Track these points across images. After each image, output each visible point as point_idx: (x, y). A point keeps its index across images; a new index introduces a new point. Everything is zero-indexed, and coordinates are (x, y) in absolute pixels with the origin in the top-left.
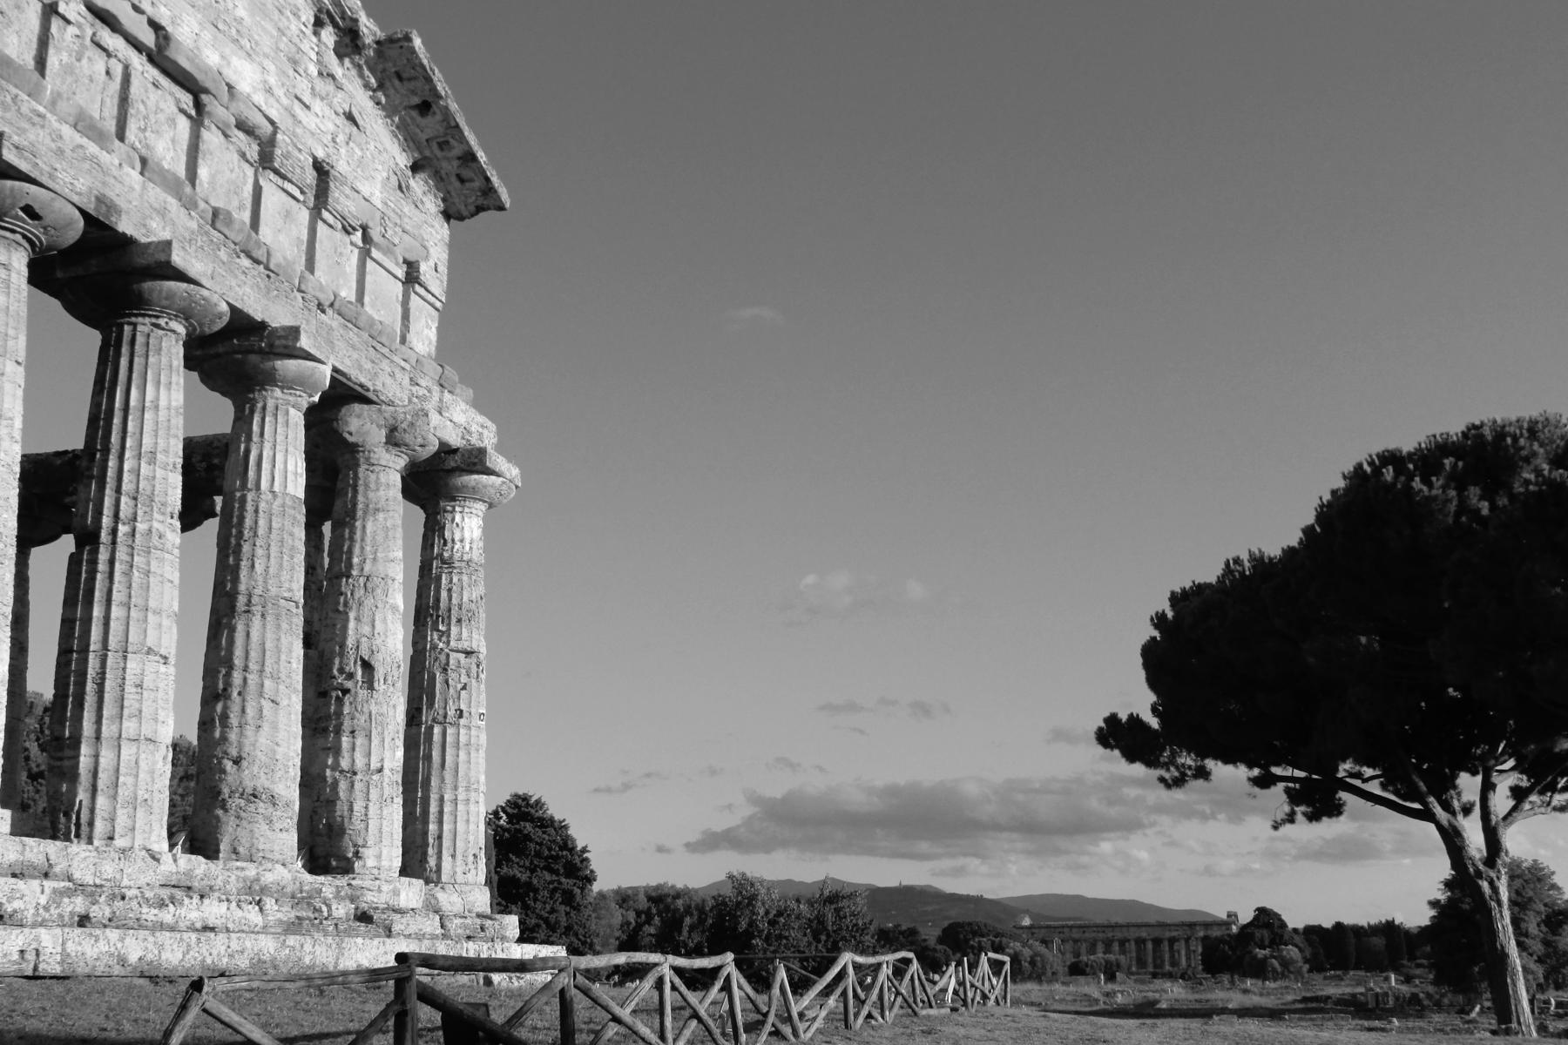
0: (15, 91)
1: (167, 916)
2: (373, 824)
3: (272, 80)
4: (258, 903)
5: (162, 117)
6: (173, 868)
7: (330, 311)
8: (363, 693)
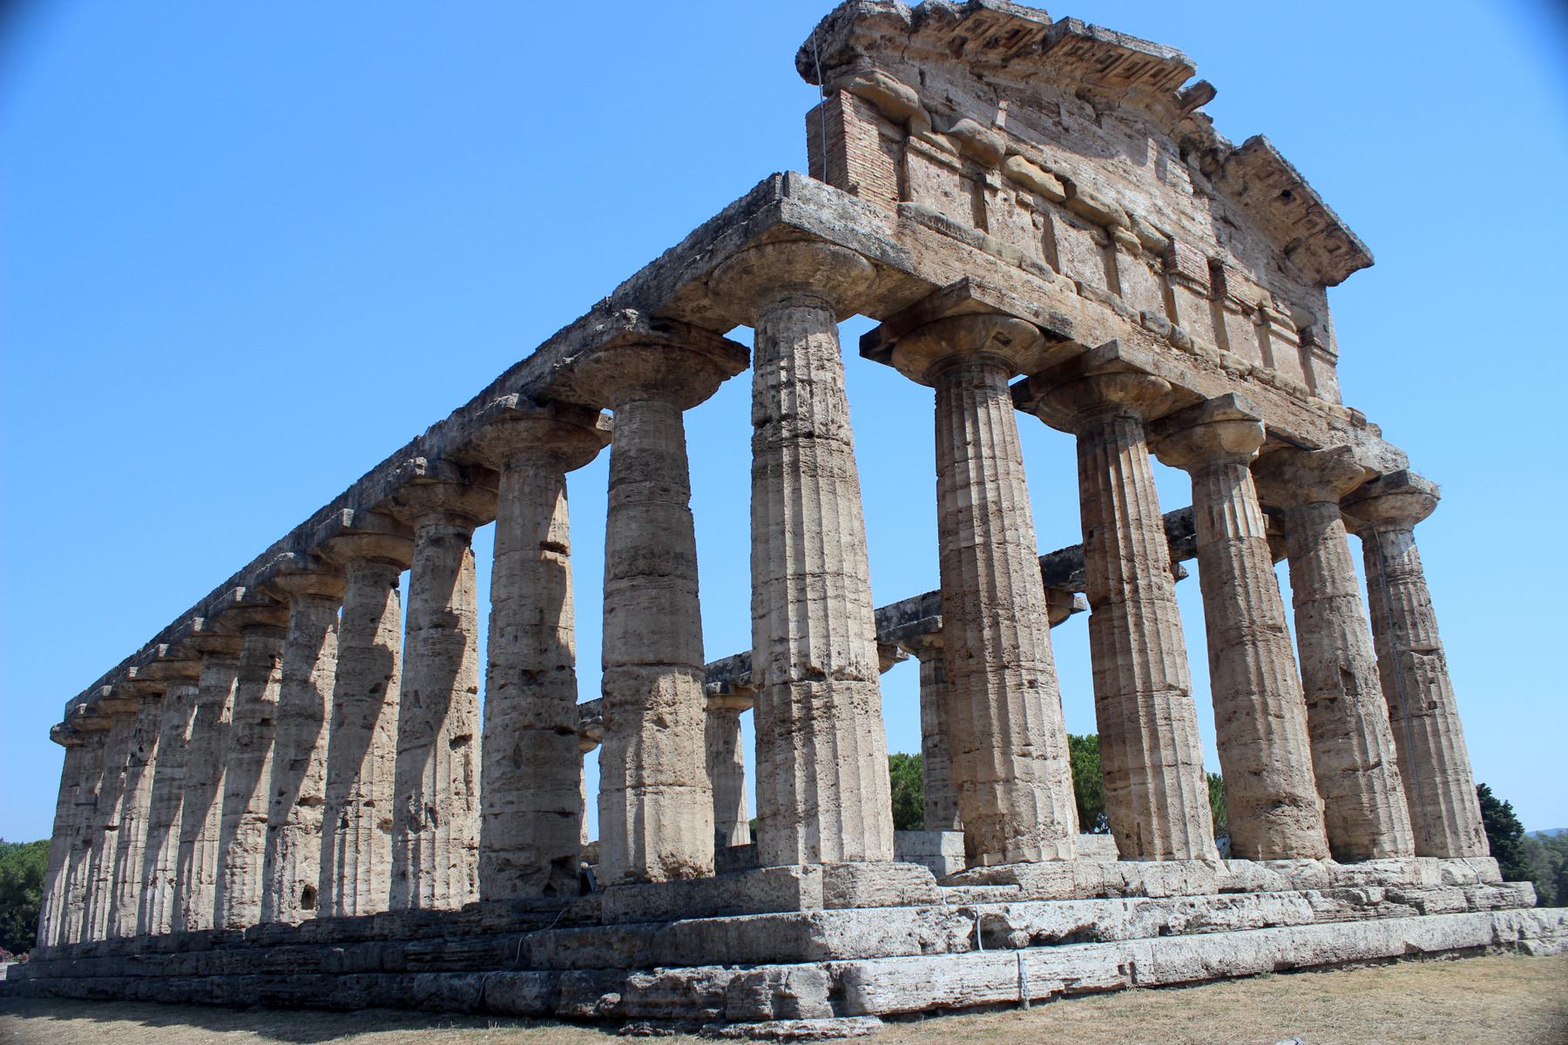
1: (1232, 916)
2: (1382, 812)
3: (1160, 203)
4: (1306, 896)
6: (1227, 873)
7: (1250, 378)
8: (1349, 699)
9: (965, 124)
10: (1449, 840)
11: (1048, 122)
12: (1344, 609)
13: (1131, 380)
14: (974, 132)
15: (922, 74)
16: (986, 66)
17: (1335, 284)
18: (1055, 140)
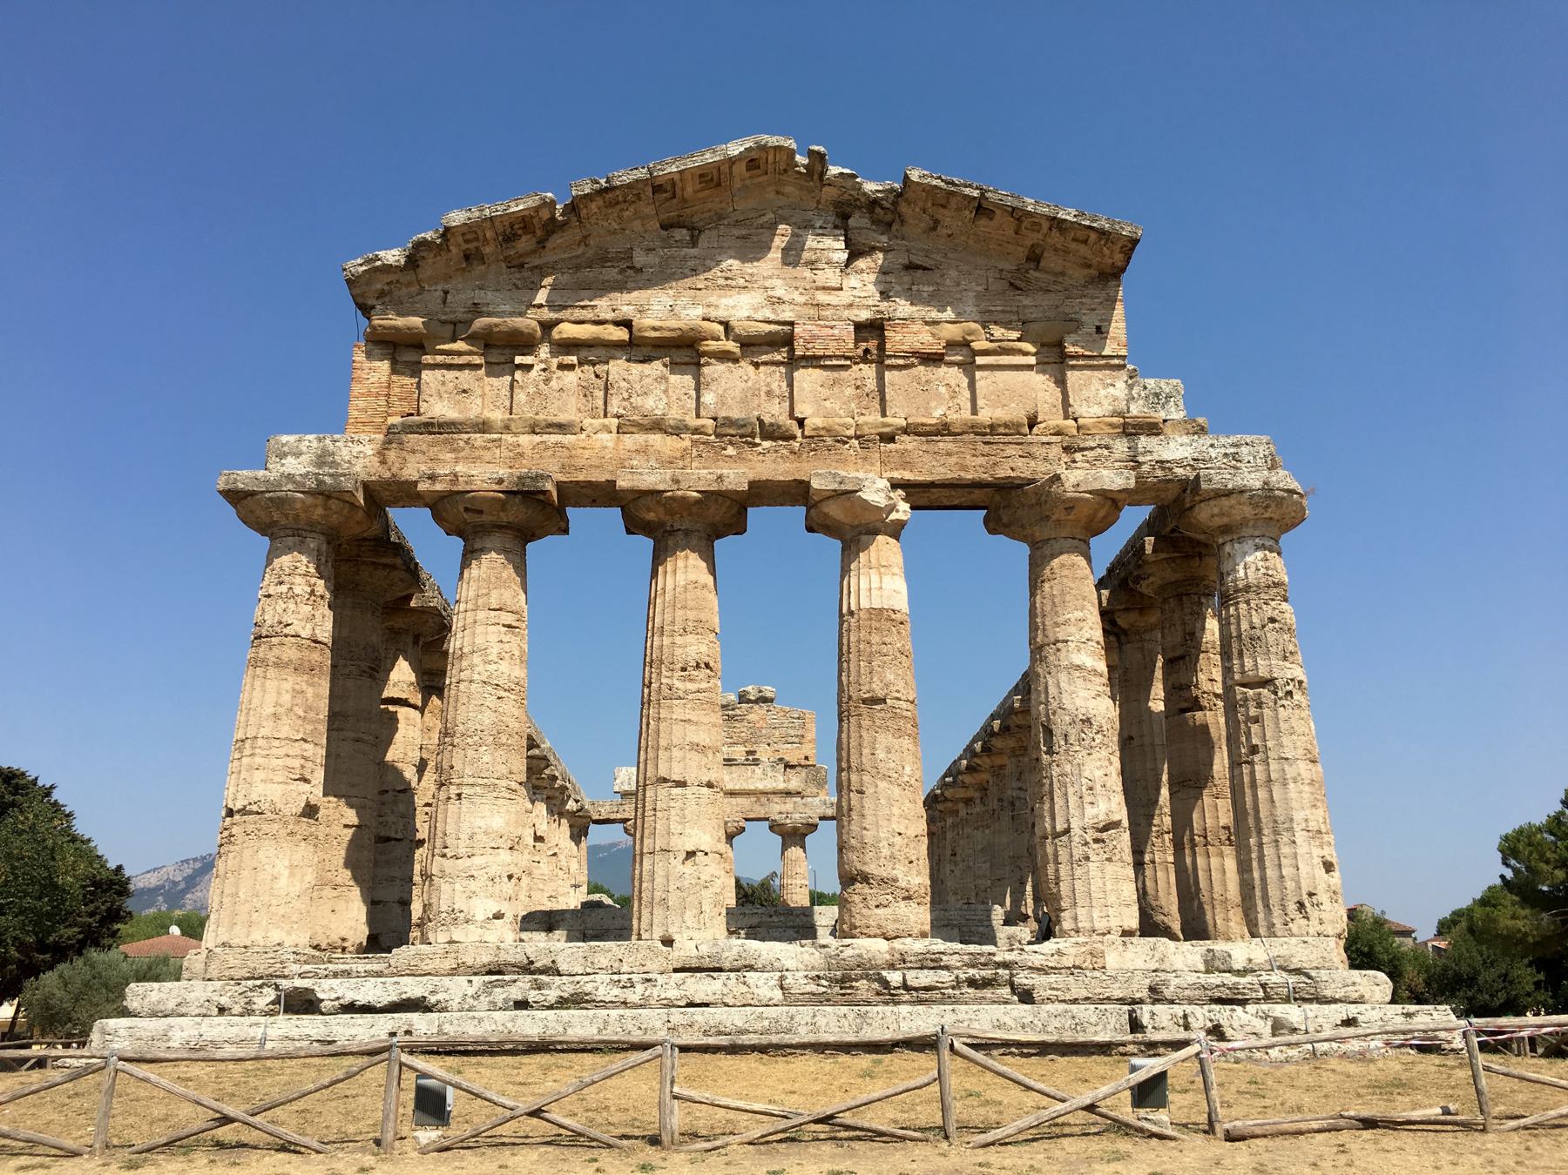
0: (465, 436)
2: (1064, 888)
3: (780, 292)
5: (649, 380)
9: (480, 323)
10: (1261, 916)
11: (612, 274)
12: (1052, 658)
13: (648, 500)
14: (490, 326)
15: (446, 293)
17: (1123, 270)
18: (621, 287)
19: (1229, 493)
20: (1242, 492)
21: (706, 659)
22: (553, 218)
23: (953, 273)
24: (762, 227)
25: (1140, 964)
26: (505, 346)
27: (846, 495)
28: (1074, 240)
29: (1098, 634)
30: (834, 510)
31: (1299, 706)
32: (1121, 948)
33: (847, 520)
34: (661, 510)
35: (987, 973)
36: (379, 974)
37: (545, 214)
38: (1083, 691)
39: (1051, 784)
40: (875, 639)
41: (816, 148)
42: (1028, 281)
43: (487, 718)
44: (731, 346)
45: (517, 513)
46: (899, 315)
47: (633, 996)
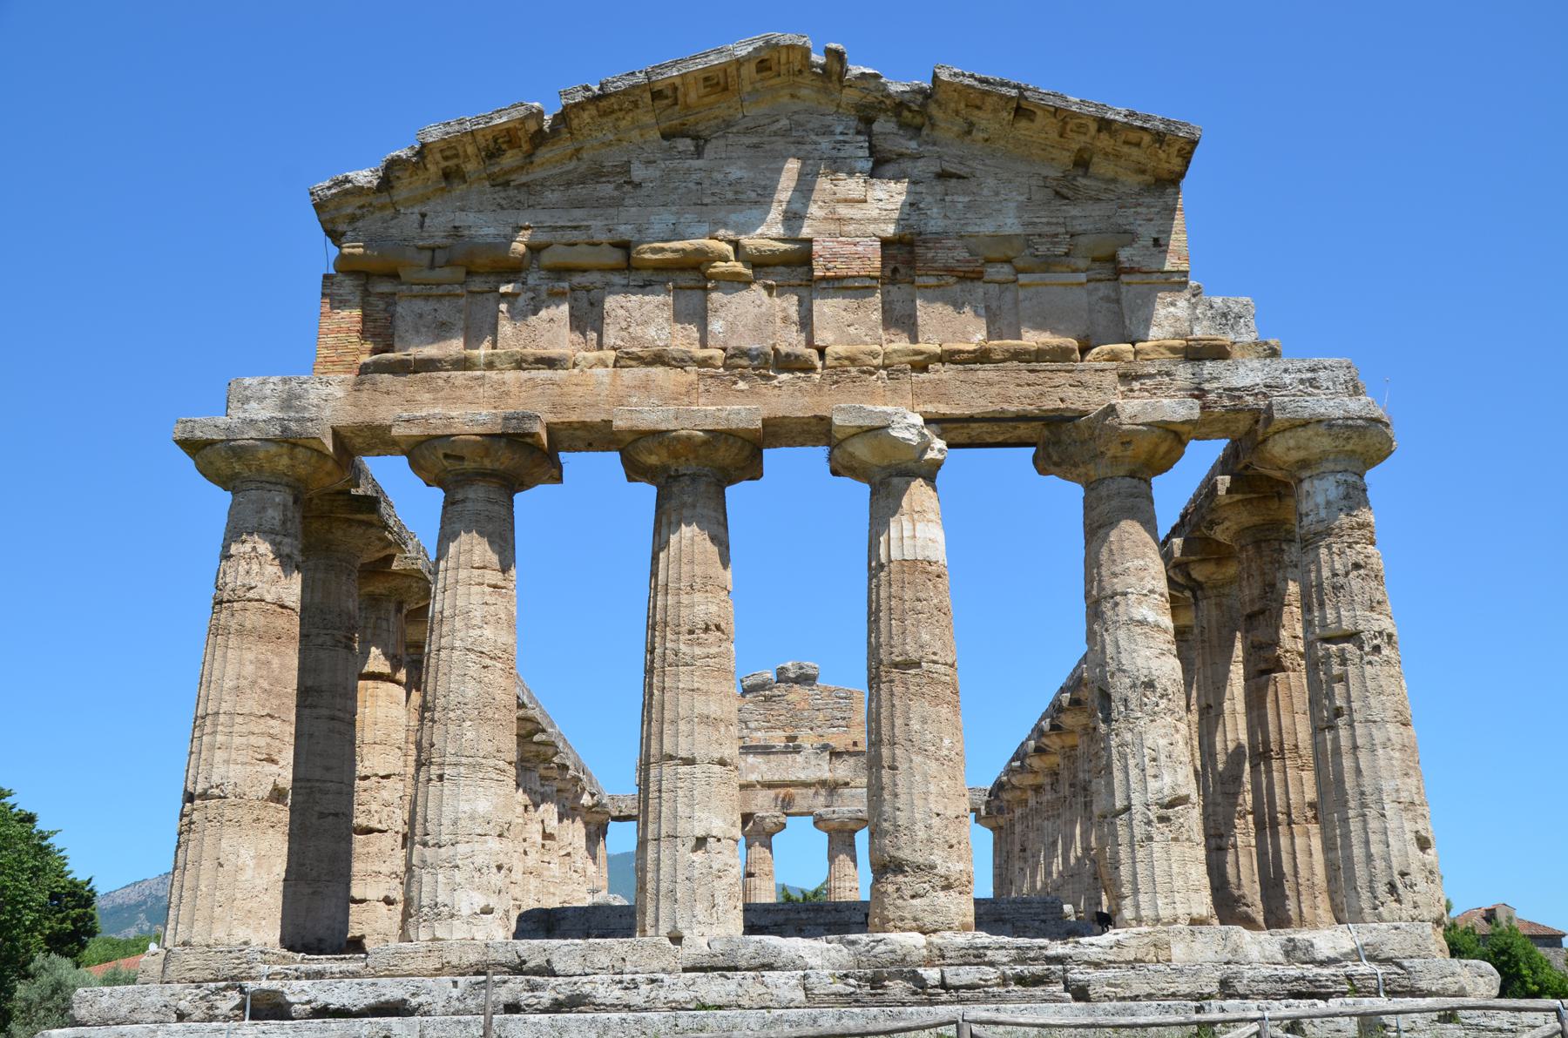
0: (444, 374)
2: (1125, 872)
8: (1103, 727)
11: (607, 190)
15: (423, 215)
16: (506, 173)
17: (1182, 175)
19: (1306, 424)
20: (1320, 421)
21: (717, 620)
22: (541, 130)
23: (991, 182)
24: (775, 134)
25: (1210, 955)
26: (489, 274)
27: (876, 432)
28: (1126, 143)
29: (1162, 585)
30: (861, 450)
31: (1388, 662)
32: (1189, 938)
33: (874, 461)
34: (664, 453)
35: (1038, 969)
36: (354, 974)
37: (532, 126)
38: (1149, 651)
39: (1110, 756)
40: (908, 594)
41: (833, 45)
42: (1076, 189)
43: (471, 690)
44: (739, 267)
45: (505, 459)
46: (930, 229)
47: (636, 998)
